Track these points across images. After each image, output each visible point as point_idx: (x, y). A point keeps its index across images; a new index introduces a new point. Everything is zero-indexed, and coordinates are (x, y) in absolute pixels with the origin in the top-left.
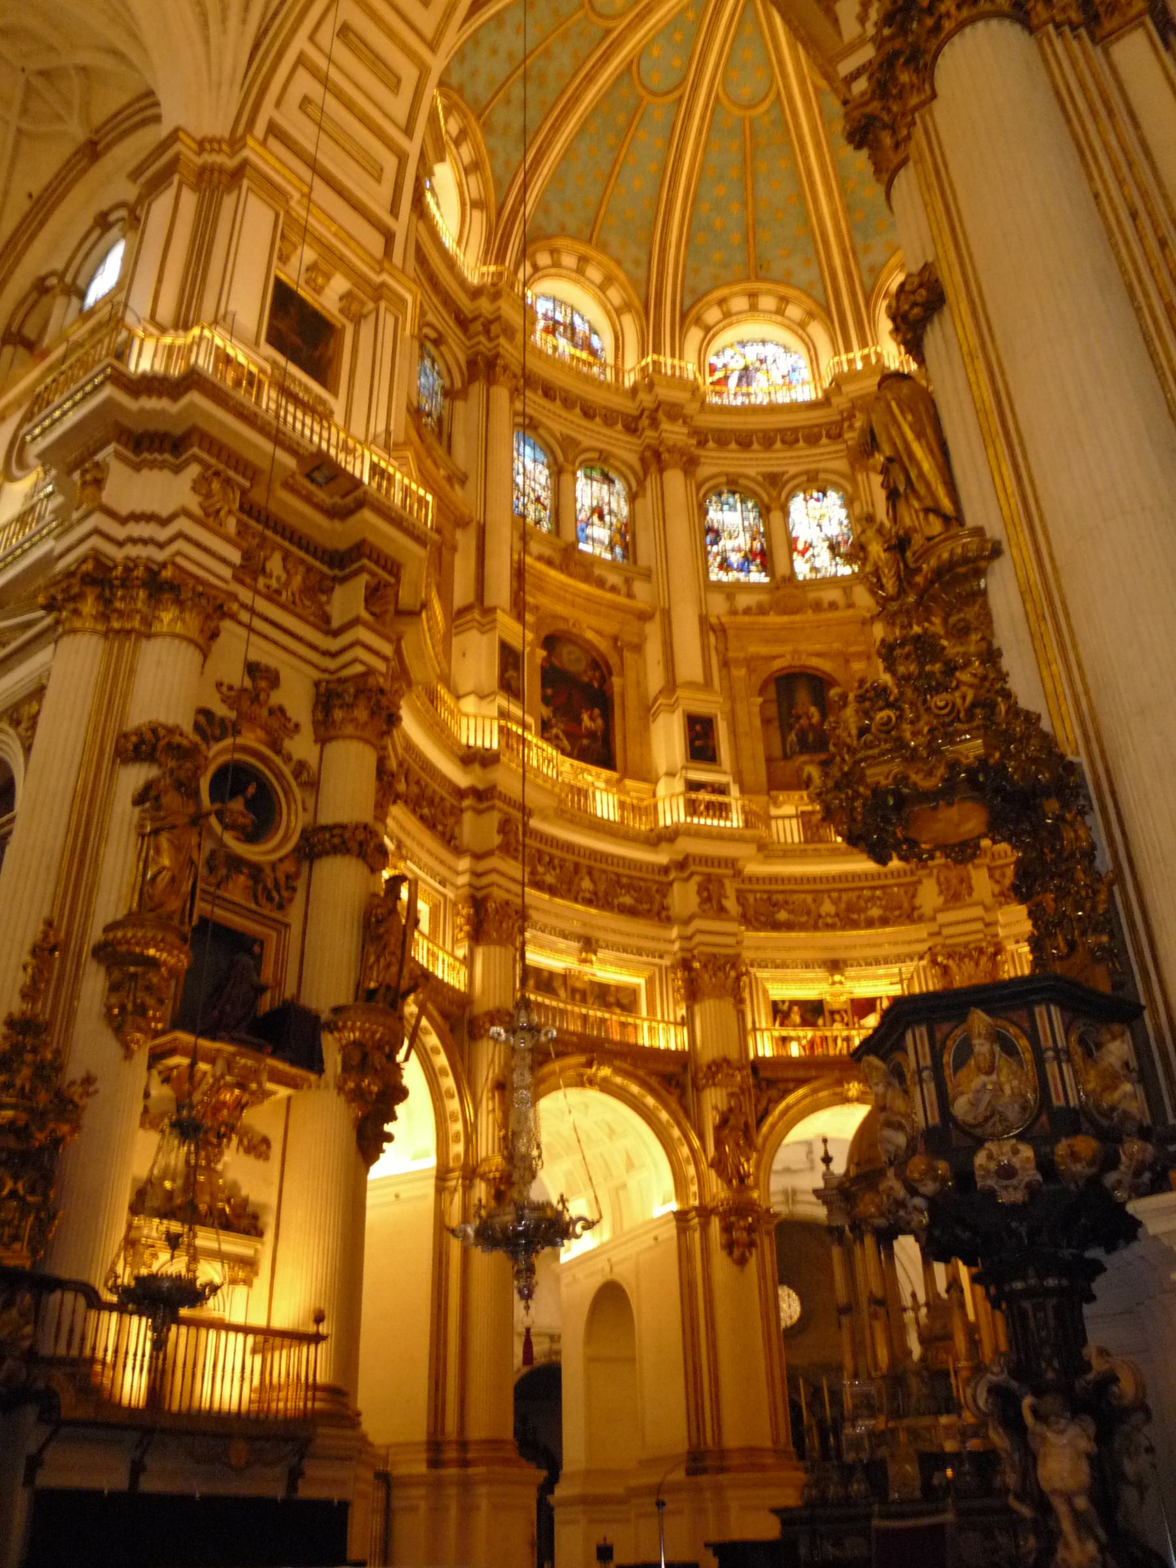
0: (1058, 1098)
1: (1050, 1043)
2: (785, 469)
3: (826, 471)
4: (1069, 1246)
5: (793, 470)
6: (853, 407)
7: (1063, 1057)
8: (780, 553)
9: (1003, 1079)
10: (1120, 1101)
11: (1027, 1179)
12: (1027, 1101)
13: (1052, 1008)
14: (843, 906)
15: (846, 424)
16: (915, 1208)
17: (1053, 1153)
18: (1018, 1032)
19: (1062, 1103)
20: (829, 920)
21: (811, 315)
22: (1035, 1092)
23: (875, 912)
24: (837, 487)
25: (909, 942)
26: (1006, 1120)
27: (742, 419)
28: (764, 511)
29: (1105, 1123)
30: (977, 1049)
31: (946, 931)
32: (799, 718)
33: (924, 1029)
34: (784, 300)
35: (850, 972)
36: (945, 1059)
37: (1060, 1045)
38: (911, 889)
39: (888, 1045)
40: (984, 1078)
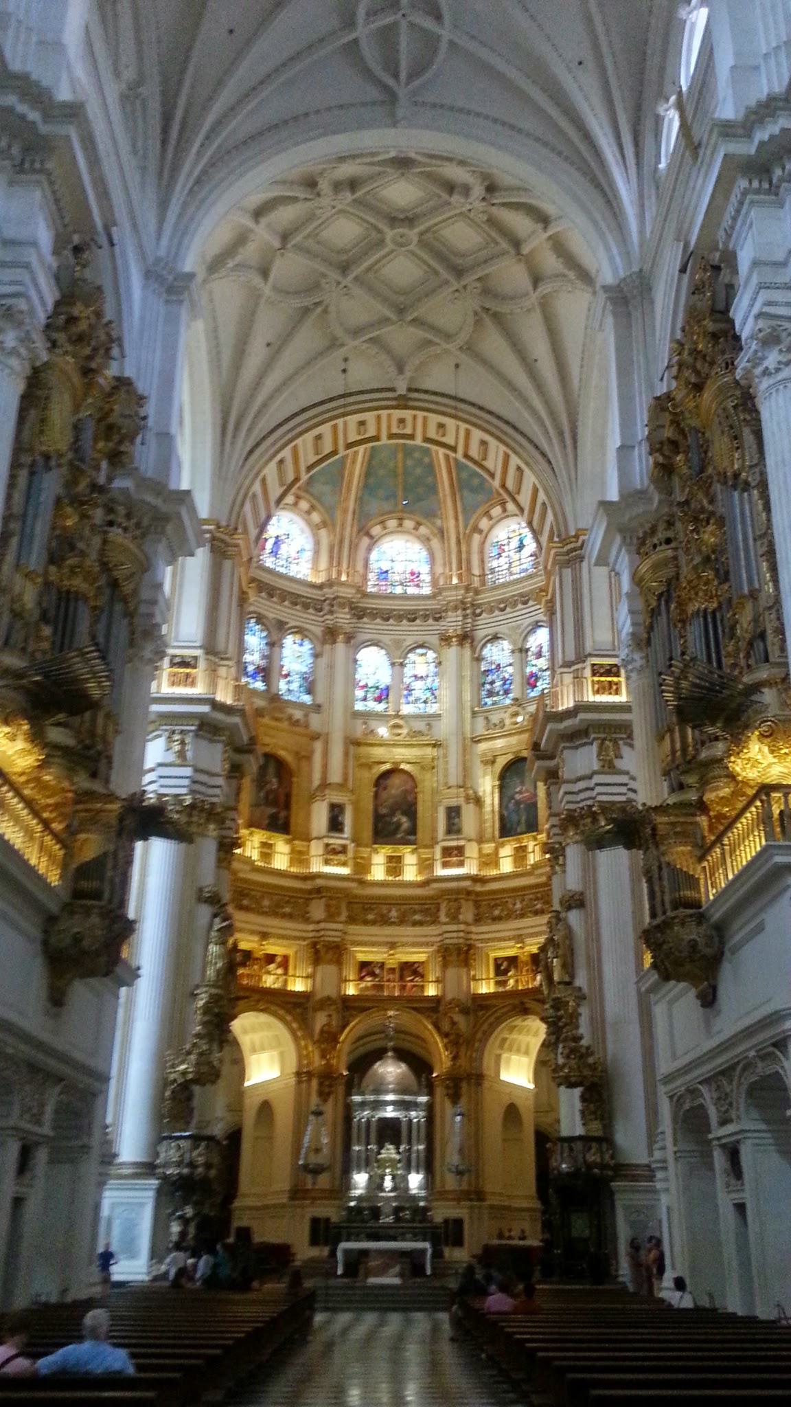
2: (287, 620)
3: (310, 631)
5: (292, 624)
6: (334, 599)
8: (275, 674)
15: (326, 608)
20: (265, 909)
21: (324, 524)
23: (287, 910)
24: (311, 641)
27: (269, 576)
28: (271, 645)
31: (322, 933)
32: (267, 783)
34: (313, 508)
35: (272, 940)
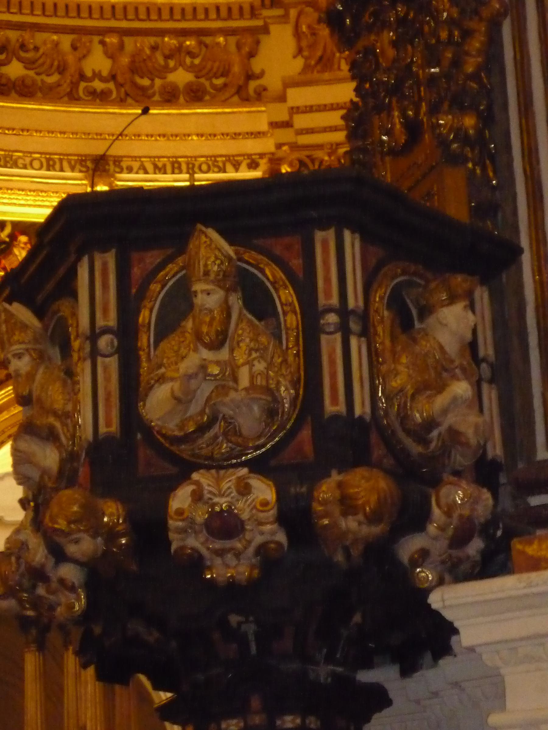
0: (335, 400)
1: (335, 301)
4: (330, 659)
7: (354, 326)
9: (240, 357)
10: (445, 412)
11: (259, 540)
12: (276, 399)
13: (347, 235)
14: (125, 60)
16: (62, 581)
17: (310, 496)
18: (280, 274)
19: (341, 408)
20: (98, 85)
22: (295, 384)
25: (236, 136)
26: (238, 433)
29: (416, 449)
30: (200, 300)
31: (300, 121)
33: (111, 258)
36: (144, 316)
37: (351, 303)
38: (249, 40)
39: (50, 286)
40: (206, 354)
